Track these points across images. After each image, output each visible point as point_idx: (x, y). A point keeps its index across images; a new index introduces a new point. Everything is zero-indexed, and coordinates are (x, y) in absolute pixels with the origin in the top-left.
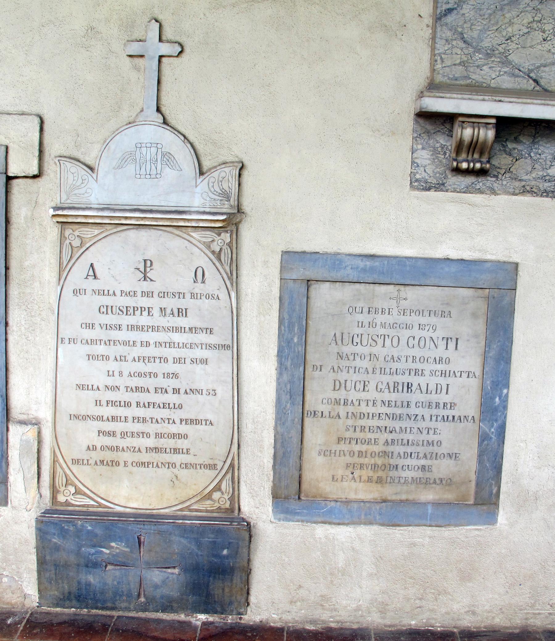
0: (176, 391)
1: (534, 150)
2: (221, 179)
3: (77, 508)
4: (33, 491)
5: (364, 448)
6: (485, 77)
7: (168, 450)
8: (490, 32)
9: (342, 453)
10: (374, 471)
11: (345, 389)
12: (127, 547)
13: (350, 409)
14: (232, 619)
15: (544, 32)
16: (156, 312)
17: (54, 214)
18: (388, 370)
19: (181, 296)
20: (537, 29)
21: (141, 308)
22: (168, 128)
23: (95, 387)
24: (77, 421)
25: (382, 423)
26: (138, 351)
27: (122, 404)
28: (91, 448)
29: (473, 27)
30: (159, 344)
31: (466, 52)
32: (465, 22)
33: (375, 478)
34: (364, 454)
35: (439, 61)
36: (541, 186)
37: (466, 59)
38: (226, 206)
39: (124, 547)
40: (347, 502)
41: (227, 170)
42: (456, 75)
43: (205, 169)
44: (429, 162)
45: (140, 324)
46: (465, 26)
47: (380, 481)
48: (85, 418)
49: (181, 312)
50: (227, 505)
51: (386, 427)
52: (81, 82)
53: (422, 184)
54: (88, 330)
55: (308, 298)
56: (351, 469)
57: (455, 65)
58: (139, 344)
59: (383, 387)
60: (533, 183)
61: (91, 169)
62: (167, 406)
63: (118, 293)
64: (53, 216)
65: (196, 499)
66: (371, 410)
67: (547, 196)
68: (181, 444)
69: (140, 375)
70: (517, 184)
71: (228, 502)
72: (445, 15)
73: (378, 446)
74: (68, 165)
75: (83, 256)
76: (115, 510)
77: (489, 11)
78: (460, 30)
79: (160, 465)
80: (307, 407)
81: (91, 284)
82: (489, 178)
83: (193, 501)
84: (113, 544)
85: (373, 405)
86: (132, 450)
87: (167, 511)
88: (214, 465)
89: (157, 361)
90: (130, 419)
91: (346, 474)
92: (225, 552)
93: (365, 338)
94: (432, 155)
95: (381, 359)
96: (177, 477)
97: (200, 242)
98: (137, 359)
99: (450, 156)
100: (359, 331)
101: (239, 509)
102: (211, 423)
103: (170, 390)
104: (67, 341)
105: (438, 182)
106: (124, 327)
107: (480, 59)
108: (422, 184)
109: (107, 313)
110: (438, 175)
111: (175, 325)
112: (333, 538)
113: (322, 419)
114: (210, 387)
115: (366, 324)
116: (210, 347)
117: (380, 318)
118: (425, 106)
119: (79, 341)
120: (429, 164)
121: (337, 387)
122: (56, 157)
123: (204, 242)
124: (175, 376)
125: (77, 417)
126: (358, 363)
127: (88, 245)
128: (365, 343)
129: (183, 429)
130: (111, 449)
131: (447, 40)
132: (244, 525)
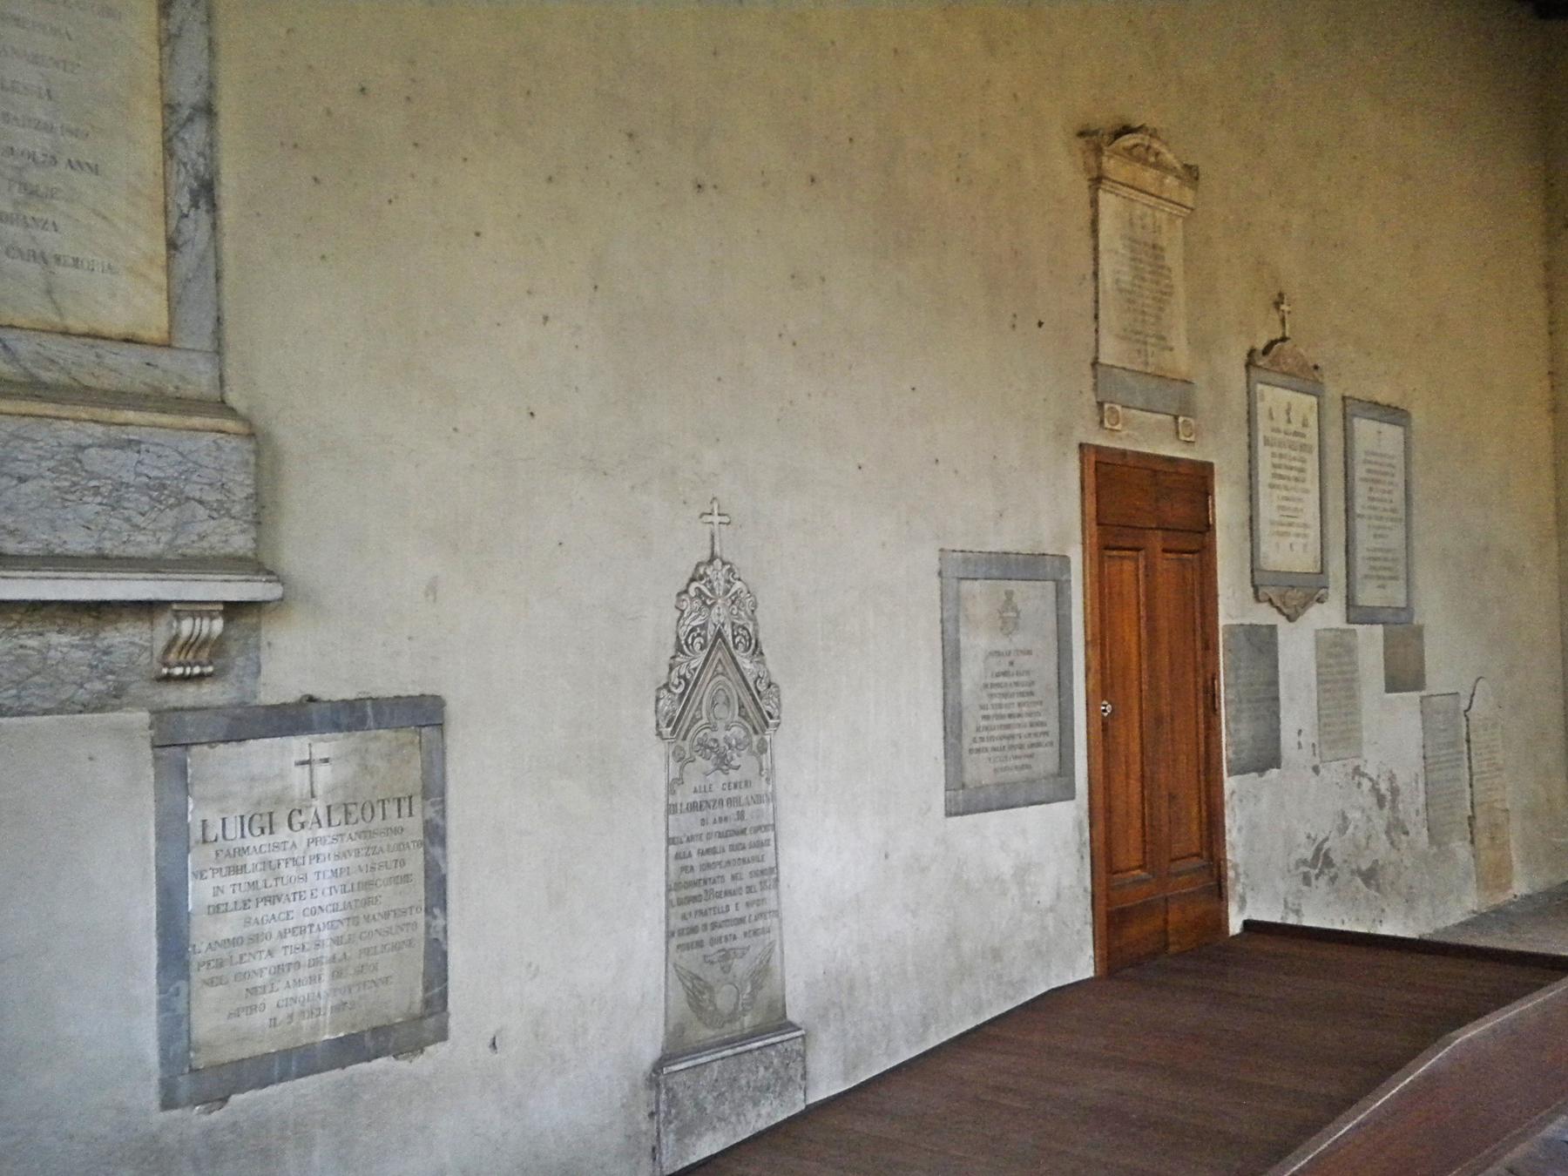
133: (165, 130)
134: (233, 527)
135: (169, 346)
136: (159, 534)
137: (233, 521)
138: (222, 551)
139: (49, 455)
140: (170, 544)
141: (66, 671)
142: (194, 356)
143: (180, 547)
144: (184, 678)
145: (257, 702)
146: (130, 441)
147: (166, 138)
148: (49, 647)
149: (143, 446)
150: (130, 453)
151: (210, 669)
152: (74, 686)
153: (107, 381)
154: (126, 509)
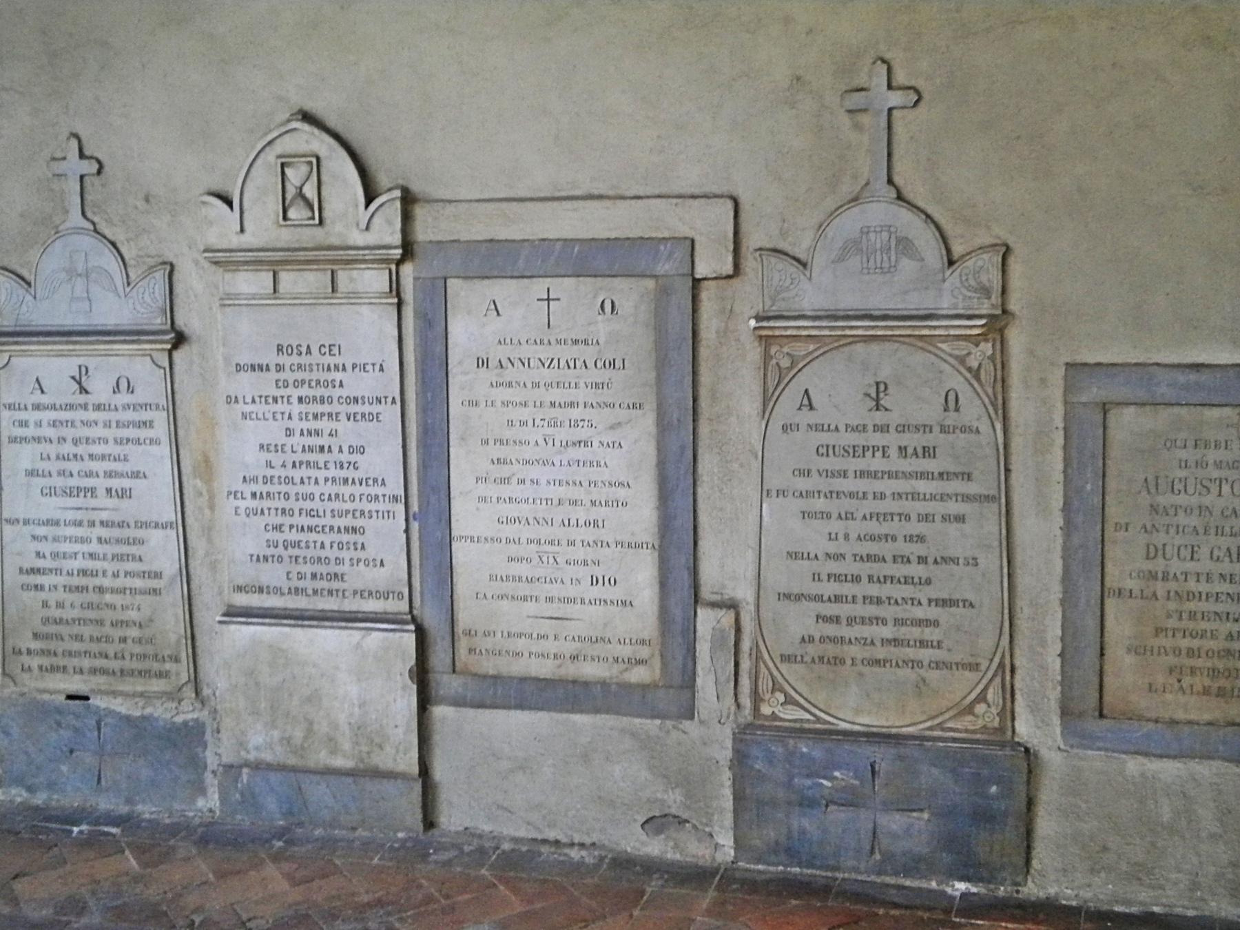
0: (922, 560)
2: (977, 269)
3: (787, 724)
4: (729, 701)
5: (1196, 643)
7: (912, 643)
9: (1162, 650)
10: (1212, 679)
11: (1165, 558)
12: (856, 778)
13: (1173, 586)
14: (1005, 890)
16: (893, 452)
17: (757, 325)
18: (1227, 530)
19: (927, 429)
21: (873, 447)
22: (905, 204)
23: (812, 555)
24: (787, 602)
25: (1220, 608)
26: (870, 506)
27: (849, 578)
28: (807, 638)
30: (898, 496)
33: (1214, 690)
34: (1196, 653)
38: (985, 306)
39: (852, 778)
40: (1173, 722)
41: (985, 256)
43: (956, 256)
45: (872, 469)
47: (1221, 693)
48: (799, 597)
49: (928, 452)
50: (996, 724)
51: (1228, 614)
52: (786, 150)
54: (802, 478)
55: (1105, 428)
56: (1176, 675)
58: (870, 496)
59: (1222, 555)
61: (804, 265)
62: (910, 581)
63: (842, 428)
64: (755, 328)
65: (951, 713)
66: (1203, 587)
68: (929, 634)
69: (872, 538)
71: (997, 719)
73: (1216, 642)
74: (774, 260)
75: (794, 381)
76: (839, 728)
79: (900, 663)
80: (1108, 584)
81: (806, 417)
83: (947, 716)
84: (837, 774)
85: (1207, 581)
86: (862, 642)
87: (911, 730)
88: (977, 665)
89: (896, 518)
90: (859, 599)
91: (1170, 682)
92: (994, 789)
93: (1191, 482)
95: (1216, 512)
96: (924, 681)
97: (951, 355)
98: (868, 517)
100: (1182, 473)
101: (1014, 731)
102: (971, 605)
103: (914, 559)
104: (774, 493)
106: (851, 474)
109: (828, 455)
111: (920, 469)
112: (1154, 778)
113: (1130, 600)
114: (969, 554)
115: (1191, 463)
116: (967, 498)
117: (1212, 455)
119: (791, 493)
121: (1152, 555)
122: (756, 250)
123: (956, 357)
124: (921, 539)
125: (788, 596)
126: (1182, 519)
127: (800, 365)
128: (1190, 491)
129: (932, 612)
130: (833, 640)
132: (1021, 751)
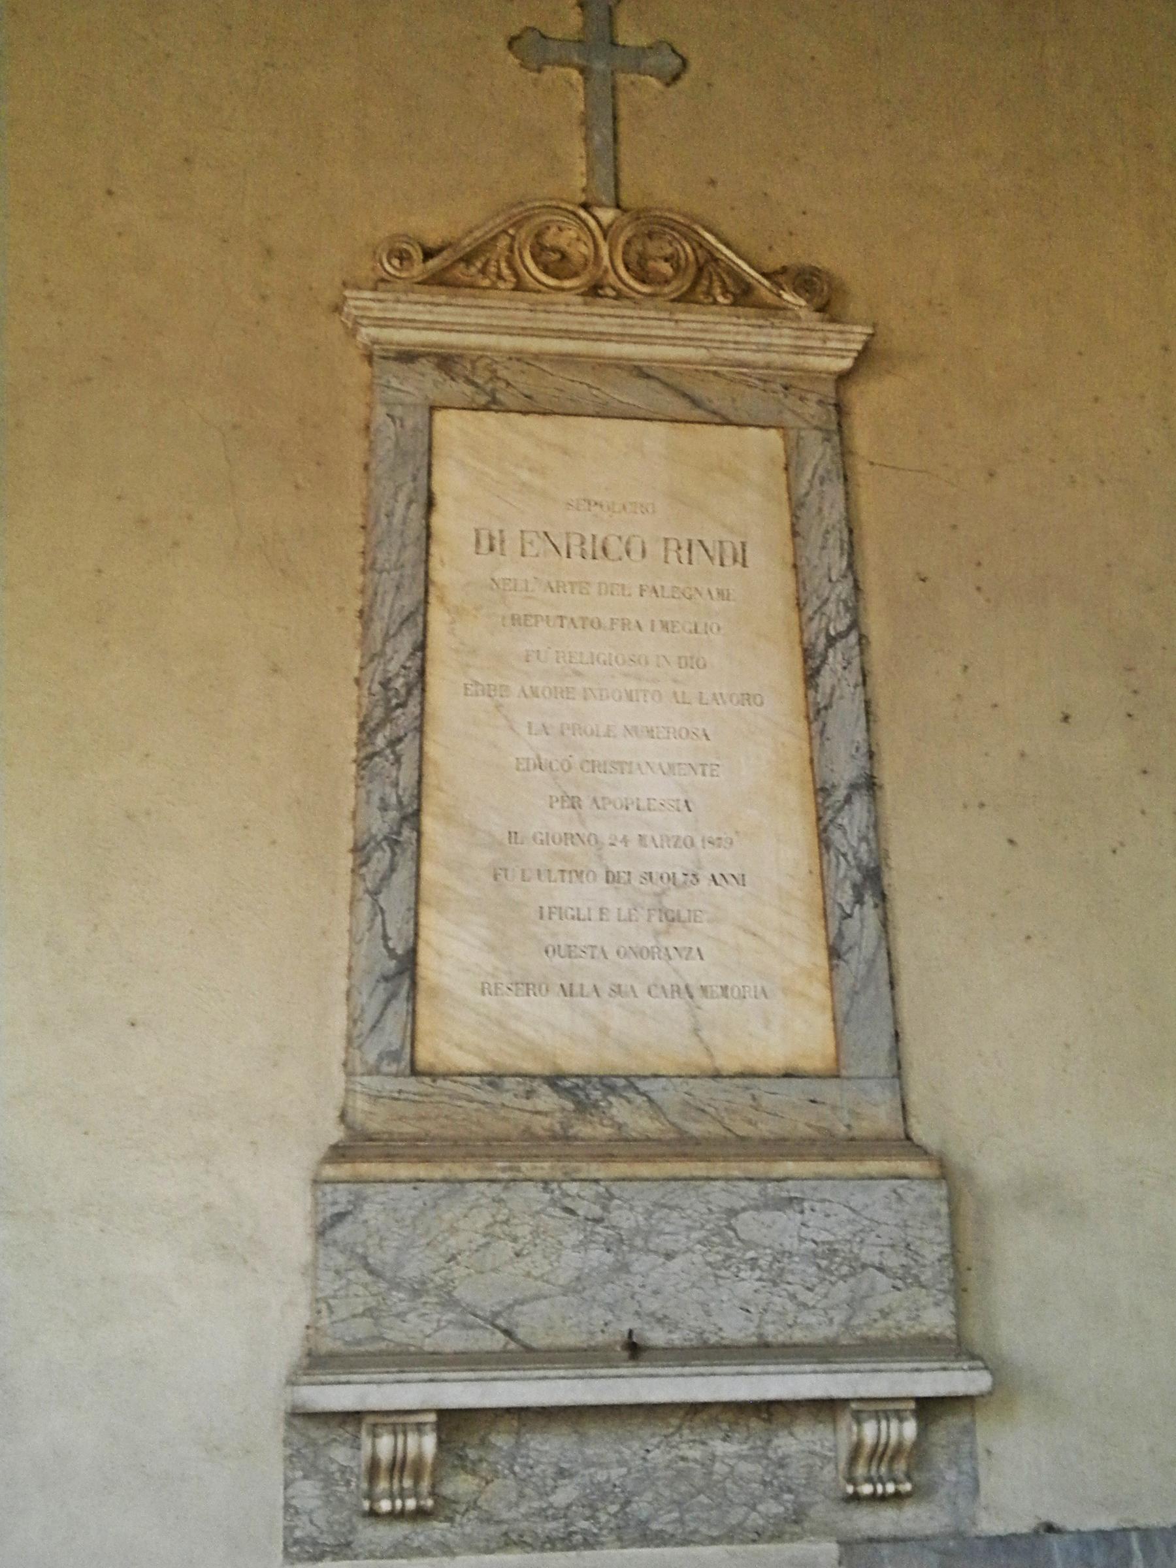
1: (519, 1460)
6: (411, 1334)
8: (416, 1251)
15: (515, 1239)
20: (502, 1236)
29: (385, 1243)
31: (374, 1290)
32: (369, 1236)
35: (325, 1313)
36: (539, 1531)
37: (374, 1304)
42: (359, 1336)
44: (319, 1503)
46: (370, 1242)
53: (307, 1548)
57: (354, 1316)
60: (524, 1525)
67: (553, 1549)
70: (492, 1530)
72: (332, 1226)
77: (413, 1212)
78: (360, 1250)
82: (436, 1524)
94: (323, 1489)
99: (358, 1486)
105: (337, 1543)
107: (401, 1300)
108: (307, 1548)
110: (336, 1527)
118: (299, 1402)
120: (319, 1508)
131: (337, 1272)
133: (819, 819)
134: (923, 1297)
135: (838, 1076)
136: (832, 1313)
137: (924, 1291)
138: (913, 1332)
139: (698, 1225)
140: (846, 1325)
141: (735, 1488)
142: (869, 1084)
143: (859, 1327)
144: (874, 1498)
145: (974, 1532)
146: (791, 1200)
147: (821, 827)
148: (713, 1459)
149: (806, 1205)
150: (790, 1213)
151: (907, 1487)
152: (745, 1509)
153: (767, 1128)
154: (789, 1283)
